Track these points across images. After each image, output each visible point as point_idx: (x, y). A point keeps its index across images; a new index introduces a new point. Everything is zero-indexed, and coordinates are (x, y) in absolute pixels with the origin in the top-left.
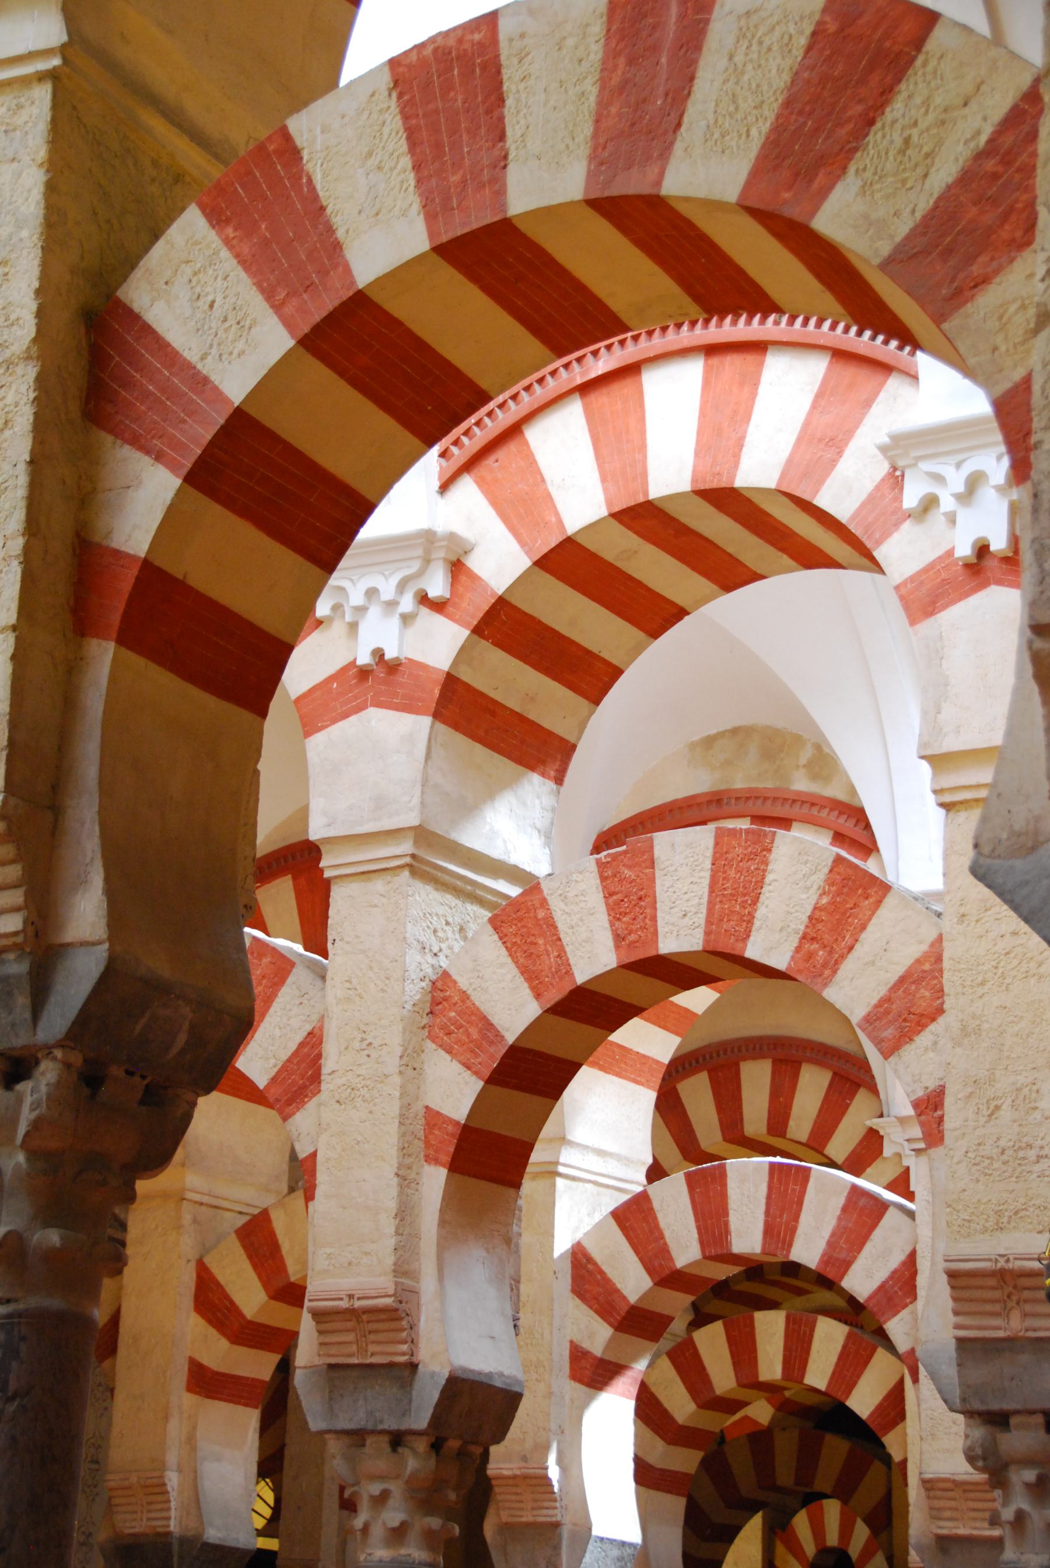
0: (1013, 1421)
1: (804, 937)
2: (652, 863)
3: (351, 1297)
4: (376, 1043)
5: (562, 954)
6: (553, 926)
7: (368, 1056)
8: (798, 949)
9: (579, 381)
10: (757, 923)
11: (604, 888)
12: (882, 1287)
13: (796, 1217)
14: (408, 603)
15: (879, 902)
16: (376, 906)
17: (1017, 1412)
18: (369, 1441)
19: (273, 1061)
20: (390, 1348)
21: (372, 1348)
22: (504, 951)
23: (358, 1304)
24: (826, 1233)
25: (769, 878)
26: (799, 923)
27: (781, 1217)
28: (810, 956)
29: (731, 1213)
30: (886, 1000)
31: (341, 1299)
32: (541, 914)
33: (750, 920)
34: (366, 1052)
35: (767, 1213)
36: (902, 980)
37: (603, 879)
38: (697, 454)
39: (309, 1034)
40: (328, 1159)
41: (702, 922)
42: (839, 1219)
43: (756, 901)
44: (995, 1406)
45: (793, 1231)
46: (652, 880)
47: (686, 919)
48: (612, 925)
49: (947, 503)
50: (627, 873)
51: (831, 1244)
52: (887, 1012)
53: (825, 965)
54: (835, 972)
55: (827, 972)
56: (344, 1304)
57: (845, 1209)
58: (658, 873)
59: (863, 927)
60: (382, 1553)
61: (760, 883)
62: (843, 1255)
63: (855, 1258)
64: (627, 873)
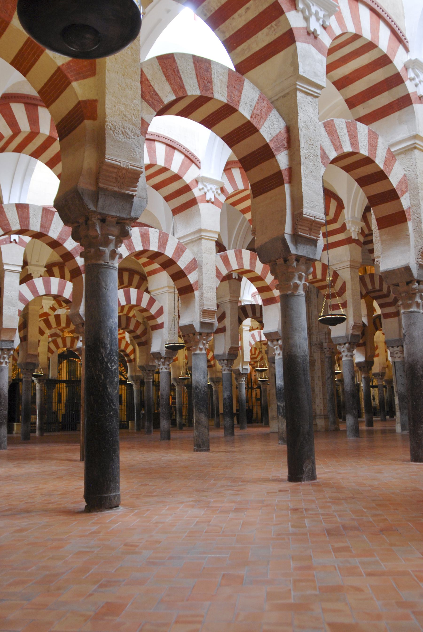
3: (314, 217)
4: (314, 145)
5: (339, 142)
6: (337, 133)
7: (312, 147)
10: (377, 155)
11: (347, 129)
14: (321, 22)
16: (309, 104)
19: (270, 136)
20: (316, 235)
21: (313, 234)
22: (326, 133)
23: (317, 220)
27: (46, 223)
28: (386, 169)
29: (30, 219)
31: (312, 217)
32: (334, 129)
34: (311, 146)
35: (42, 221)
37: (347, 127)
39: (280, 132)
40: (304, 174)
41: (367, 149)
42: (63, 227)
45: (49, 228)
47: (364, 147)
49: (417, 80)
50: (352, 128)
56: (313, 218)
62: (64, 238)
63: (68, 239)
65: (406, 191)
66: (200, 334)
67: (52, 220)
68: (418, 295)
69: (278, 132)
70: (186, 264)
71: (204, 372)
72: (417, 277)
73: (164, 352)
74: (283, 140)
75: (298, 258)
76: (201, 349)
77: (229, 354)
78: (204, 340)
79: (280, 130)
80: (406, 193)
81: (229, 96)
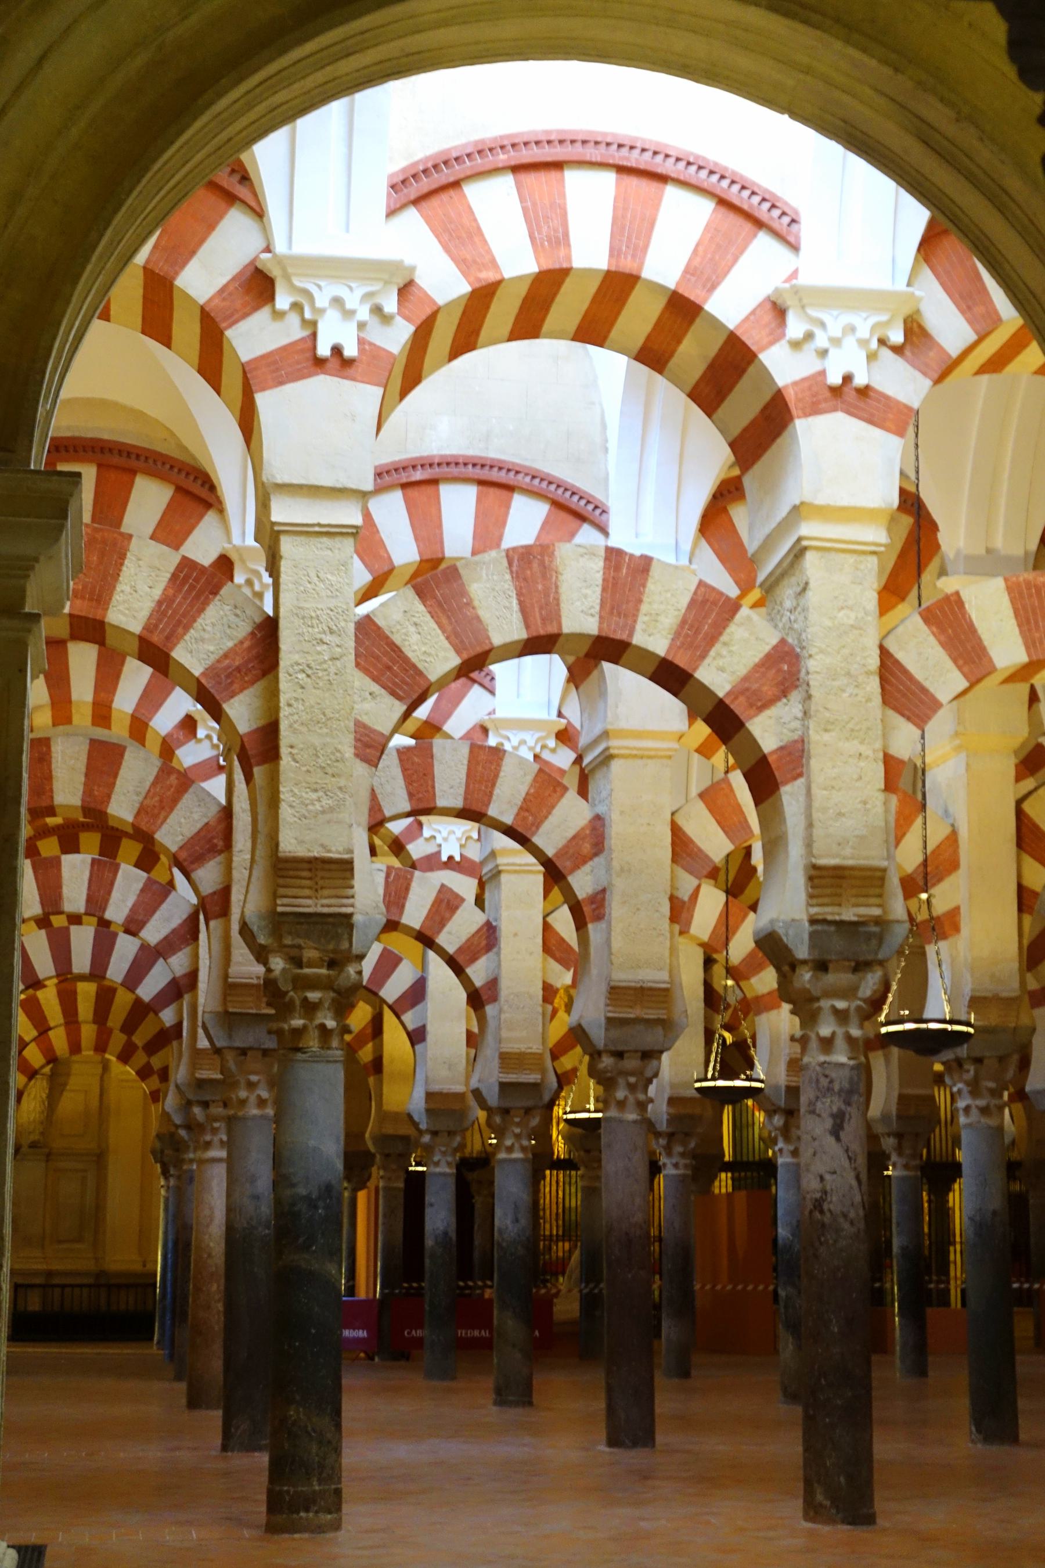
0: (626, 1055)
1: (521, 808)
2: (432, 757)
8: (517, 814)
9: (404, 480)
12: (166, 938)
13: (109, 893)
15: (562, 795)
17: (627, 1051)
18: (250, 1053)
19: (181, 837)
24: (130, 904)
25: (502, 774)
26: (519, 801)
28: (525, 819)
30: (566, 847)
33: (490, 795)
36: (574, 837)
37: (401, 760)
38: (474, 538)
43: (494, 785)
44: (620, 1048)
46: (432, 766)
48: (407, 787)
50: (416, 760)
51: (133, 910)
52: (567, 853)
53: (533, 824)
54: (538, 828)
55: (534, 829)
57: (142, 891)
58: (436, 763)
59: (553, 807)
60: (255, 1111)
61: (496, 776)
62: (140, 918)
64: (416, 760)
65: (596, 854)
66: (506, 1112)
67: (112, 884)
68: (621, 1081)
69: (199, 826)
70: (464, 939)
71: (516, 1207)
72: (606, 1045)
73: (665, 1117)
74: (213, 838)
75: (243, 1052)
76: (510, 1150)
77: (899, 1117)
78: (518, 1125)
79: (205, 820)
80: (596, 860)
81: (88, 792)
